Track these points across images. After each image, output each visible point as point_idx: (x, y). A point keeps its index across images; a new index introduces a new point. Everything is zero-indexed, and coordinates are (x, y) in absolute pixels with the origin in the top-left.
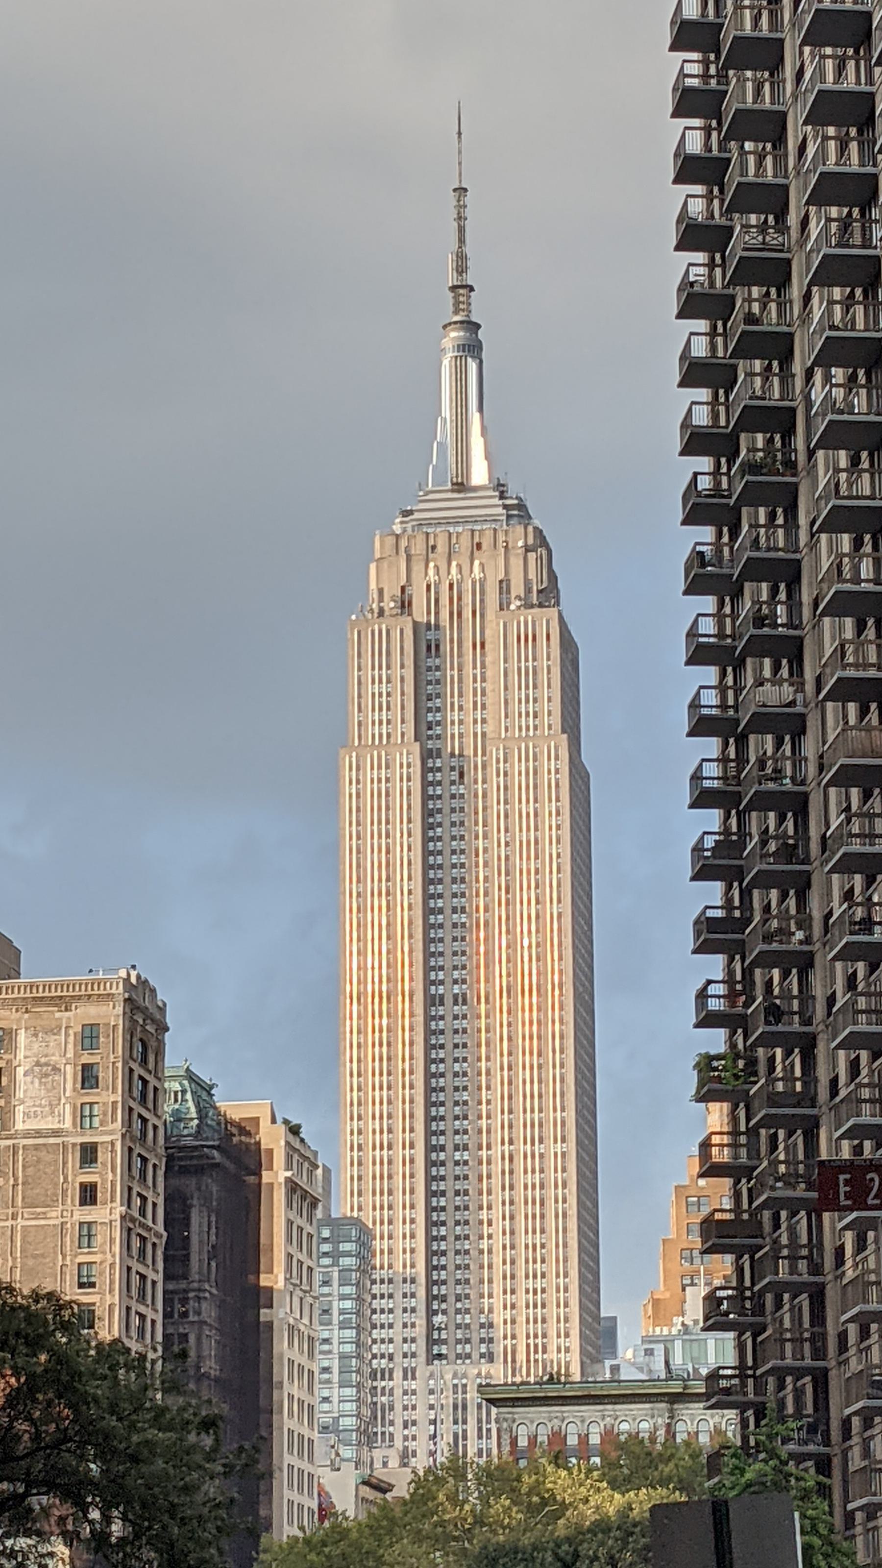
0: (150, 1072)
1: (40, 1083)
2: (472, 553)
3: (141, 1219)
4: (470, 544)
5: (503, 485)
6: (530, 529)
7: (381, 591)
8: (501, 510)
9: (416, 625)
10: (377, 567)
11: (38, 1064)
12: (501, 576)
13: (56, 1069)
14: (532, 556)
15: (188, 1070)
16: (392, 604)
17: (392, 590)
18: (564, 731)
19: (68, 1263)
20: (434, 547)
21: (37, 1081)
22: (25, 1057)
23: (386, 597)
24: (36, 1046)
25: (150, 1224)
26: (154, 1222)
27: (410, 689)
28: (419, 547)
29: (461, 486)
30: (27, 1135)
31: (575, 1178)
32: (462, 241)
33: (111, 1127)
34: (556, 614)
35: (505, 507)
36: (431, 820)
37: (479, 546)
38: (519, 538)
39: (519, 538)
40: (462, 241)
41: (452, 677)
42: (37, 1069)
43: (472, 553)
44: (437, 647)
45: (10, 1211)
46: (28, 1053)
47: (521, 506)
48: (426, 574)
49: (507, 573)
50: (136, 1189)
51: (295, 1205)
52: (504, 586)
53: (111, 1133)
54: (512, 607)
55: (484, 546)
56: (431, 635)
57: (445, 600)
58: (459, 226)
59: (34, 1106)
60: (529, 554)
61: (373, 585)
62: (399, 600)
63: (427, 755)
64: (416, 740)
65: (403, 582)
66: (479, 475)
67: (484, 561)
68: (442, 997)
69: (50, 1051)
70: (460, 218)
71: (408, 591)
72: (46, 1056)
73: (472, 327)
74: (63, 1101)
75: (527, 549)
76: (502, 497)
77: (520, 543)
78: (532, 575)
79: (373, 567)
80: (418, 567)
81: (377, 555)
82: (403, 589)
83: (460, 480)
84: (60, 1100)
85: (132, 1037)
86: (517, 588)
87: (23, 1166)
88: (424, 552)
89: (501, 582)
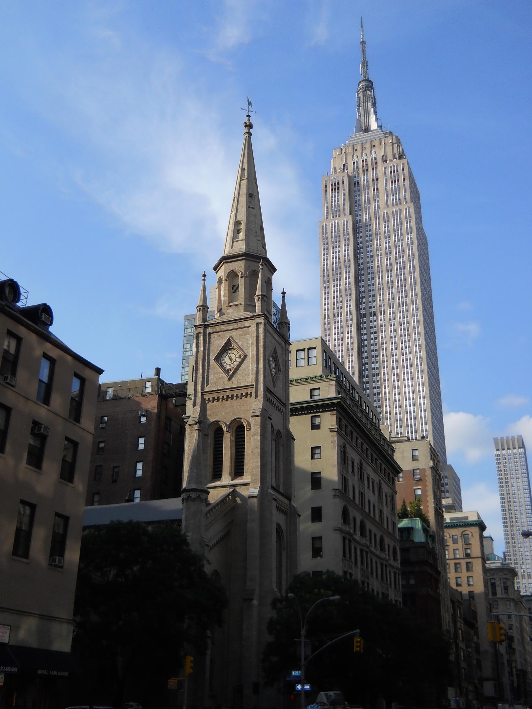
2: (371, 149)
6: (394, 137)
7: (335, 168)
9: (349, 178)
10: (334, 160)
17: (339, 166)
18: (411, 202)
23: (337, 169)
27: (347, 197)
28: (350, 150)
29: (367, 130)
31: (427, 380)
34: (406, 161)
35: (384, 133)
41: (364, 185)
43: (371, 149)
44: (358, 183)
48: (353, 159)
56: (355, 179)
58: (363, 54)
61: (332, 167)
64: (350, 214)
66: (374, 125)
67: (376, 150)
68: (365, 314)
70: (363, 51)
78: (396, 151)
79: (332, 161)
80: (349, 157)
82: (344, 165)
86: (390, 156)
89: (383, 156)
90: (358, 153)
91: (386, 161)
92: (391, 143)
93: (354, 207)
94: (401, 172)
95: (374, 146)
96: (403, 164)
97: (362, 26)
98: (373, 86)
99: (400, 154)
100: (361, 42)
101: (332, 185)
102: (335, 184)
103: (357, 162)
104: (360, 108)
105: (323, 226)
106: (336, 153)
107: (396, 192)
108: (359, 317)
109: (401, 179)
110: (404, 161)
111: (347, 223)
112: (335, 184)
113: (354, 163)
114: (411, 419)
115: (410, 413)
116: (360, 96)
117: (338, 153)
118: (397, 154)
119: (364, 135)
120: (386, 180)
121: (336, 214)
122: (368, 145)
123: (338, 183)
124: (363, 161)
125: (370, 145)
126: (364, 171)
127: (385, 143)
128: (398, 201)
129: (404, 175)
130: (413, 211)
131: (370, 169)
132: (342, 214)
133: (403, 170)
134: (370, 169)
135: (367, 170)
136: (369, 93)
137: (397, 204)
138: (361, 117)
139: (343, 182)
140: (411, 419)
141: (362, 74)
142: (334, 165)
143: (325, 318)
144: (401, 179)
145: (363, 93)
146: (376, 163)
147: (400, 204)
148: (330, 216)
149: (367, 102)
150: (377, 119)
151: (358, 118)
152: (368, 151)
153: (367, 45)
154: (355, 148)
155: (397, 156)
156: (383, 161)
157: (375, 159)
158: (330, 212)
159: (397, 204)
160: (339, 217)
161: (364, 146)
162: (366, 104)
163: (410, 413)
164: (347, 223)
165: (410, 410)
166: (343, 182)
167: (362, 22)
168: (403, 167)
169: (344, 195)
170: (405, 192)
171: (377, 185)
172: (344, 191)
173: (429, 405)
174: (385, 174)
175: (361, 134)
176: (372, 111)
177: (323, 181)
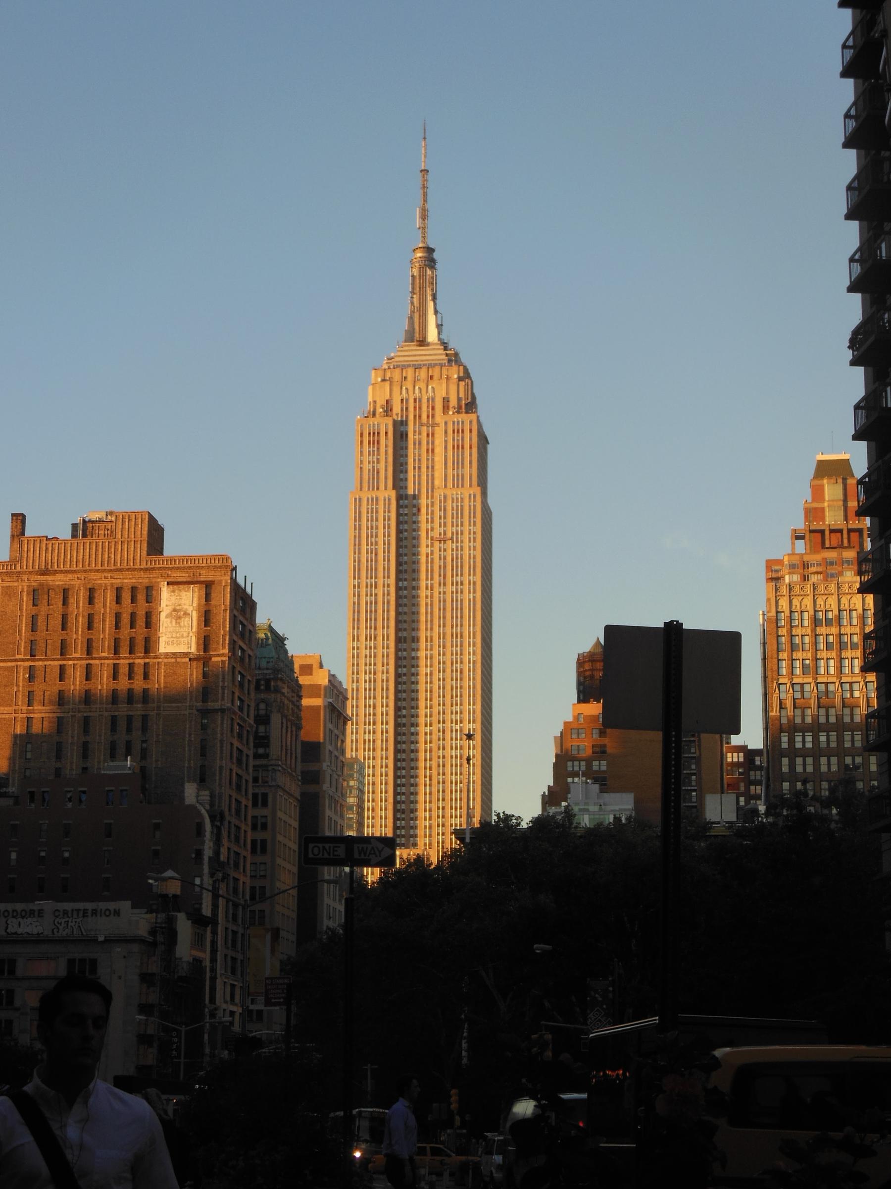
0: (247, 619)
1: (176, 622)
2: (428, 381)
3: (241, 714)
4: (426, 376)
5: (446, 343)
6: (461, 368)
8: (444, 357)
9: (395, 423)
11: (175, 610)
12: (444, 395)
13: (186, 614)
14: (462, 384)
15: (270, 625)
16: (381, 410)
17: (381, 402)
19: (193, 739)
20: (405, 378)
21: (174, 621)
22: (167, 606)
24: (173, 598)
25: (246, 718)
26: (248, 716)
29: (423, 342)
30: (167, 655)
31: (480, 744)
32: (425, 201)
33: (221, 652)
35: (447, 355)
37: (432, 377)
38: (455, 373)
39: (455, 373)
40: (425, 201)
42: (174, 613)
45: (155, 705)
46: (169, 603)
47: (456, 355)
49: (447, 393)
50: (237, 694)
51: (334, 721)
52: (446, 401)
53: (223, 655)
54: (451, 413)
55: (435, 378)
56: (402, 429)
57: (411, 408)
58: (424, 192)
59: (172, 637)
60: (460, 382)
63: (399, 498)
64: (393, 489)
65: (388, 397)
66: (432, 335)
67: (434, 386)
68: (405, 638)
69: (183, 602)
72: (180, 605)
73: (430, 250)
74: (191, 634)
75: (460, 379)
76: (445, 349)
77: (456, 376)
78: (462, 395)
80: (396, 389)
81: (373, 382)
82: (387, 402)
83: (421, 339)
84: (189, 634)
85: (235, 595)
86: (453, 402)
87: (164, 676)
90: (409, 384)
91: (448, 408)
96: (471, 422)
97: (425, 138)
99: (467, 399)
100: (421, 171)
101: (370, 433)
102: (374, 433)
103: (407, 400)
104: (415, 296)
105: (355, 499)
106: (376, 377)
107: (458, 463)
109: (467, 446)
110: (473, 417)
111: (389, 500)
112: (374, 433)
113: (402, 400)
114: (456, 791)
115: (456, 784)
116: (415, 274)
118: (463, 398)
119: (418, 350)
120: (446, 441)
122: (423, 374)
123: (378, 433)
124: (415, 400)
125: (426, 374)
129: (471, 439)
132: (382, 486)
133: (471, 431)
136: (429, 272)
137: (458, 487)
138: (414, 312)
140: (456, 791)
141: (419, 228)
142: (373, 397)
143: (354, 640)
144: (467, 446)
145: (420, 270)
146: (433, 408)
147: (462, 486)
149: (426, 288)
150: (439, 326)
151: (411, 314)
152: (423, 385)
153: (430, 176)
154: (404, 375)
155: (464, 402)
156: (444, 407)
159: (458, 487)
161: (417, 374)
162: (423, 291)
163: (456, 784)
164: (389, 500)
165: (456, 779)
166: (386, 433)
167: (425, 130)
170: (471, 467)
171: (433, 443)
172: (387, 444)
173: (480, 776)
174: (446, 432)
175: (413, 346)
176: (431, 305)
177: (358, 426)
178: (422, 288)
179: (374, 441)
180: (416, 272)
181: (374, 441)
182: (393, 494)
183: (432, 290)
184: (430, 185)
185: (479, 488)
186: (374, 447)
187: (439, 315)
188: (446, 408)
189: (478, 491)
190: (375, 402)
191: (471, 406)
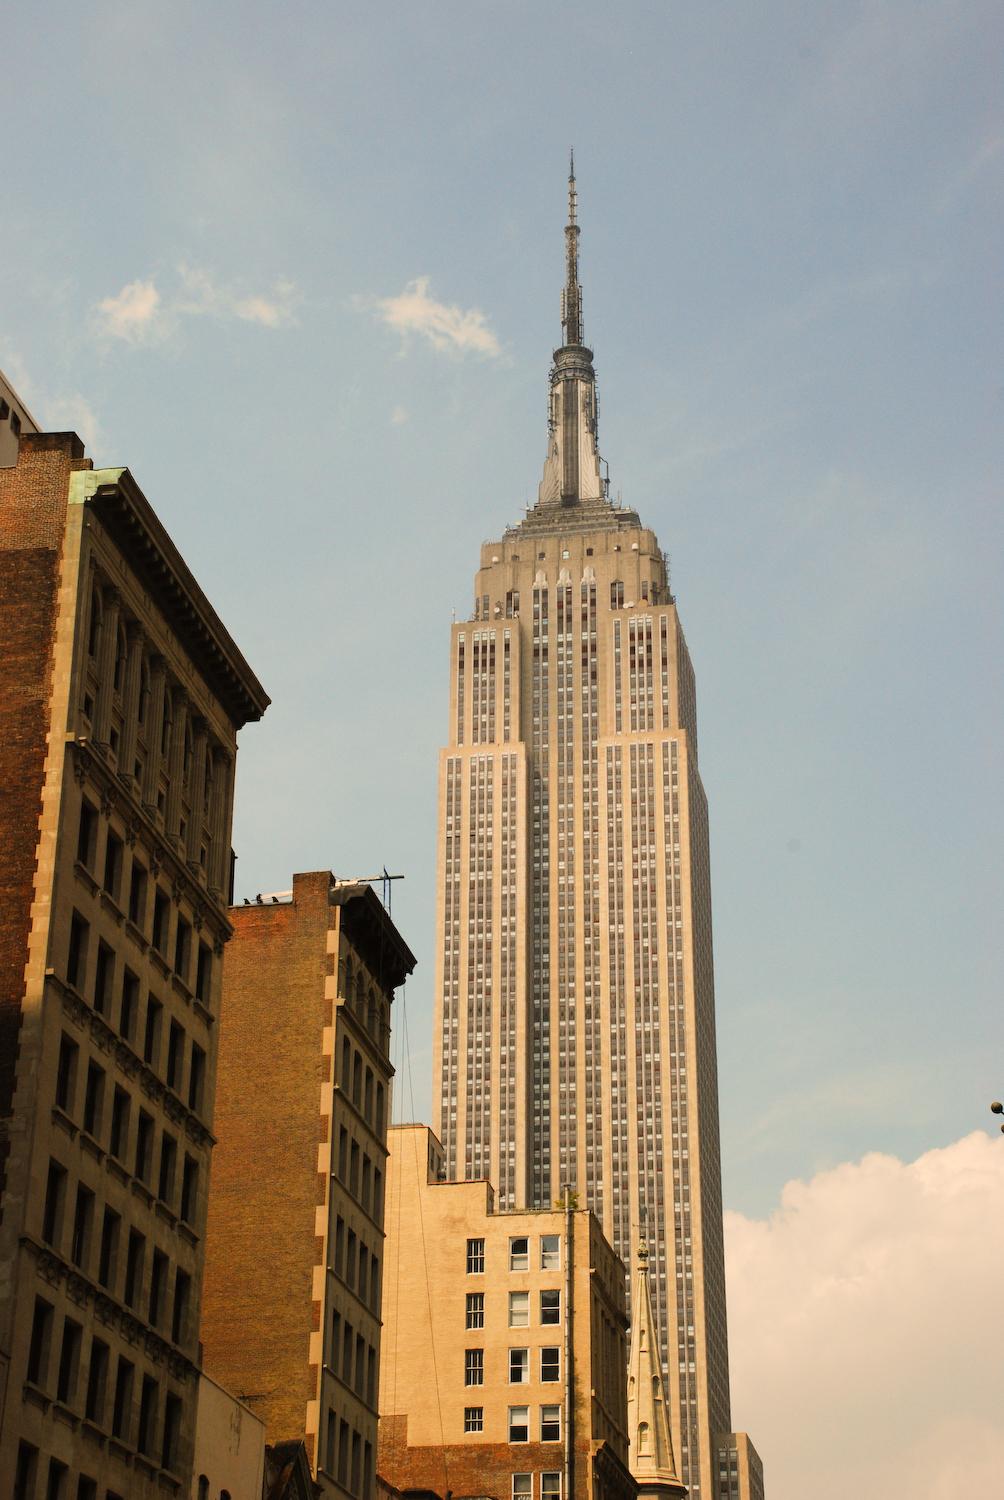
4: (580, 550)
6: (644, 534)
20: (542, 555)
23: (492, 603)
27: (515, 690)
29: (570, 499)
32: (572, 250)
34: (673, 612)
36: (537, 826)
37: (590, 552)
60: (641, 557)
62: (504, 606)
64: (521, 739)
71: (515, 595)
80: (526, 573)
82: (509, 596)
83: (570, 493)
88: (533, 558)
89: (613, 585)
91: (621, 601)
92: (635, 550)
93: (531, 714)
94: (656, 641)
95: (590, 552)
96: (663, 619)
98: (594, 364)
101: (476, 649)
102: (484, 648)
108: (532, 1018)
110: (665, 612)
112: (484, 648)
113: (536, 593)
117: (495, 559)
121: (484, 734)
123: (493, 648)
126: (560, 618)
127: (619, 549)
128: (643, 719)
130: (682, 751)
131: (577, 617)
132: (499, 736)
134: (577, 617)
135: (569, 618)
139: (507, 647)
144: (657, 661)
146: (593, 602)
148: (468, 734)
153: (581, 239)
156: (613, 600)
157: (593, 591)
158: (469, 724)
159: (642, 727)
160: (492, 741)
168: (664, 626)
169: (507, 682)
172: (506, 672)
178: (570, 414)
179: (484, 662)
180: (559, 389)
181: (484, 662)
182: (518, 750)
183: (589, 416)
184: (580, 251)
185: (683, 731)
186: (484, 671)
187: (603, 465)
188: (617, 600)
189: (680, 737)
190: (486, 599)
191: (659, 594)
